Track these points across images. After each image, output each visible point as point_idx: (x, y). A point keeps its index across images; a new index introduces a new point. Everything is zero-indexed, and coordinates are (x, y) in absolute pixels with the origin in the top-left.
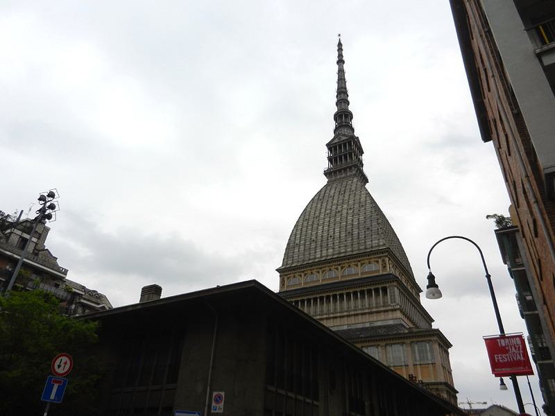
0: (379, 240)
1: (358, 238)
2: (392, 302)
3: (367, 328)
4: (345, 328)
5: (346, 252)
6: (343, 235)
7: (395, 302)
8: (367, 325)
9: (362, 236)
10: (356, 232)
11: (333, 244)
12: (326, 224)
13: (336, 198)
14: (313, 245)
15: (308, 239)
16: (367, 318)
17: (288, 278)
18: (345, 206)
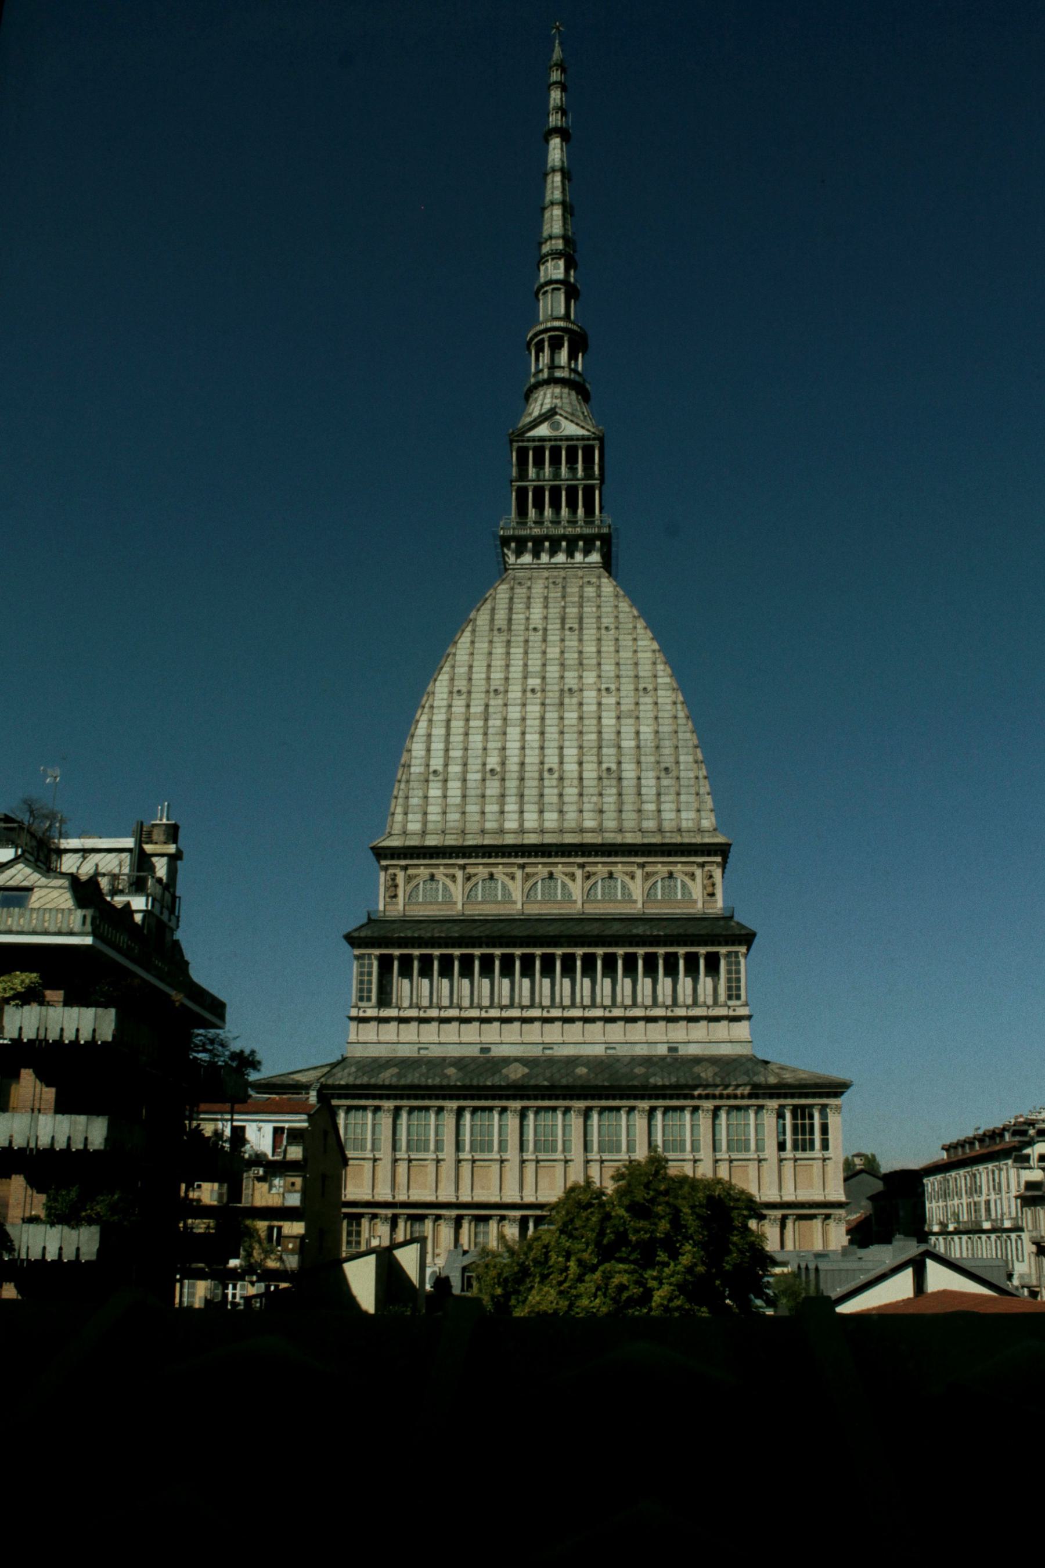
0: (698, 811)
1: (640, 794)
2: (730, 997)
3: (663, 1058)
4: (599, 1050)
5: (601, 830)
6: (590, 773)
7: (738, 997)
8: (662, 1050)
9: (649, 789)
10: (629, 771)
11: (561, 795)
12: (533, 723)
13: (554, 637)
14: (493, 788)
15: (474, 765)
16: (657, 1032)
17: (409, 879)
18: (590, 678)
